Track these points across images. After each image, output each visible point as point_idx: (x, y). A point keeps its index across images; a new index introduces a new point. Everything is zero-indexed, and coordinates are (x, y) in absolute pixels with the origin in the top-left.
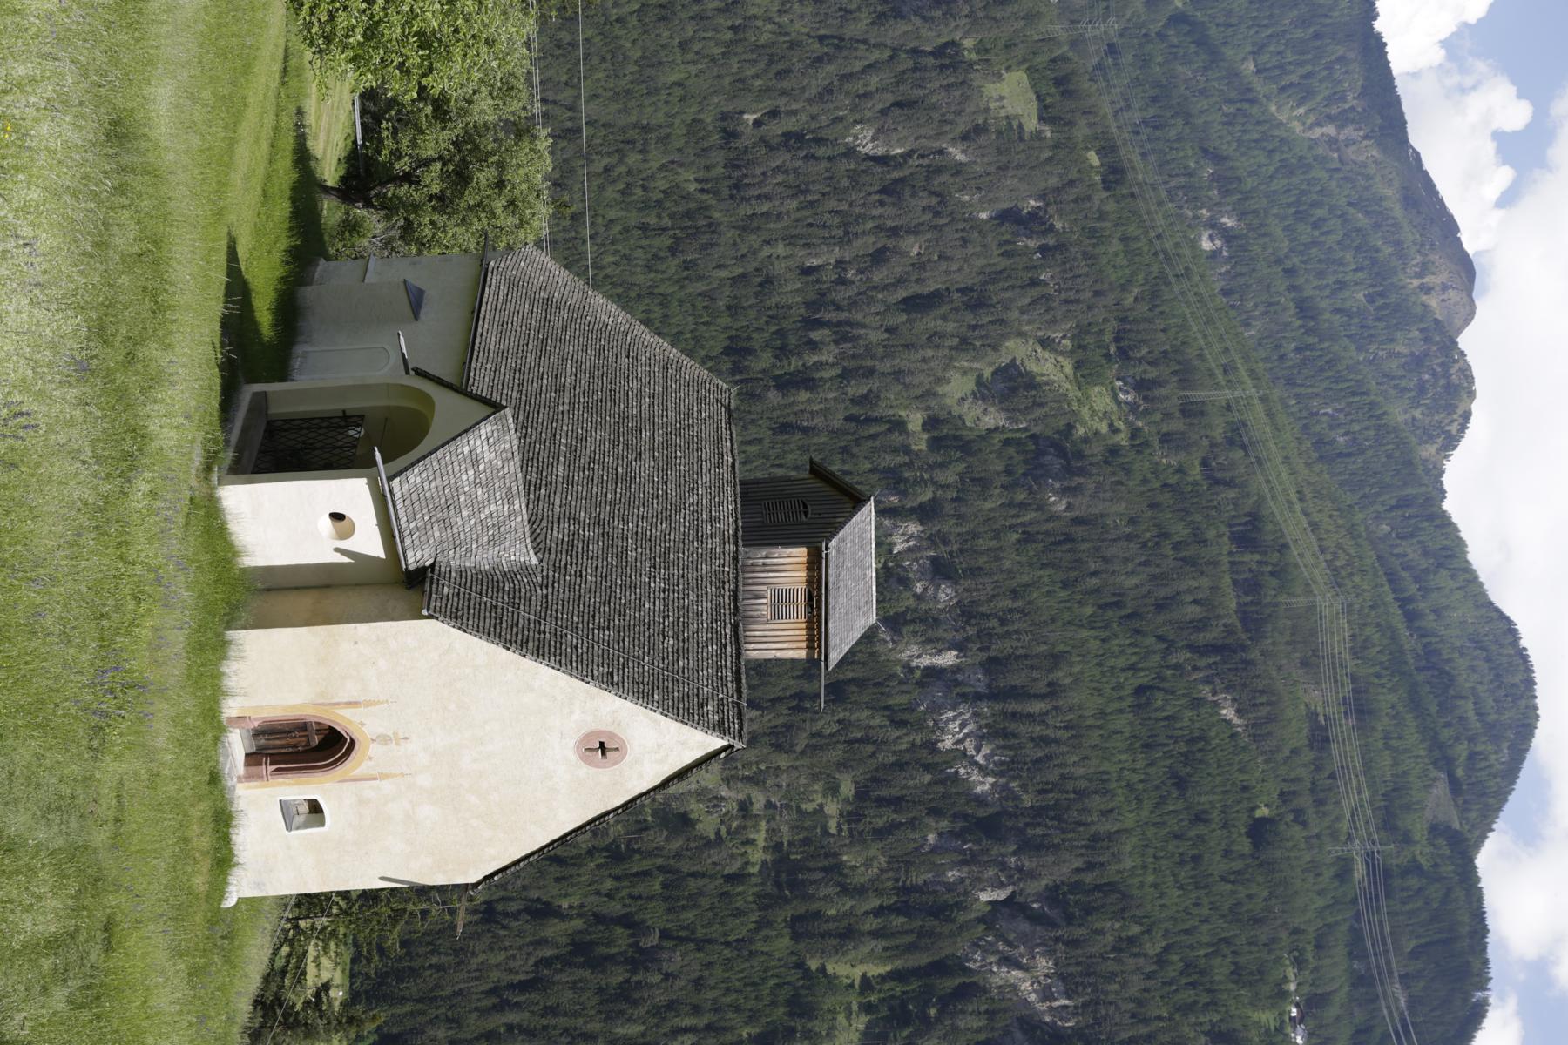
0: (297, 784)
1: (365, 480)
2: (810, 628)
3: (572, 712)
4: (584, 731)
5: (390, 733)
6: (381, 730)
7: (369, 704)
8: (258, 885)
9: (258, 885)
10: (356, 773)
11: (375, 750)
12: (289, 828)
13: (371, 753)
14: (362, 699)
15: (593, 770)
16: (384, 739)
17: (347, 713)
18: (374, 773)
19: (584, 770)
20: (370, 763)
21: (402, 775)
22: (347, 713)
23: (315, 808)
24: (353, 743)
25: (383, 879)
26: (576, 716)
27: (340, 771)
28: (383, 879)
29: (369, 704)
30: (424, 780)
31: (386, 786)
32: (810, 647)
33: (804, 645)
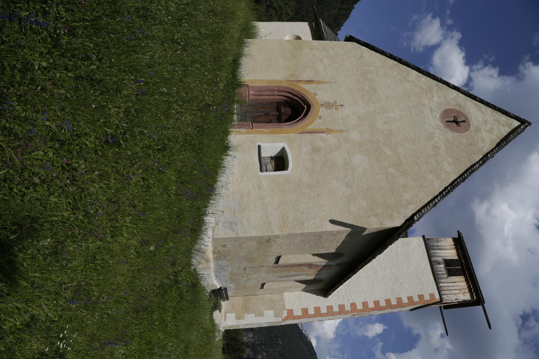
0: (272, 133)
1: (307, 23)
2: (466, 280)
3: (433, 96)
4: (443, 109)
5: (332, 102)
6: (326, 99)
7: (319, 82)
8: (231, 225)
9: (231, 225)
10: (311, 127)
11: (322, 112)
12: (261, 170)
13: (320, 114)
14: (315, 79)
15: (456, 134)
16: (328, 105)
17: (307, 87)
18: (324, 128)
19: (450, 135)
20: (320, 121)
21: (341, 131)
22: (307, 87)
23: (280, 162)
24: (309, 107)
25: (333, 222)
26: (435, 99)
27: (301, 124)
28: (333, 222)
29: (319, 82)
30: (355, 136)
31: (331, 138)
32: (470, 291)
33: (467, 291)
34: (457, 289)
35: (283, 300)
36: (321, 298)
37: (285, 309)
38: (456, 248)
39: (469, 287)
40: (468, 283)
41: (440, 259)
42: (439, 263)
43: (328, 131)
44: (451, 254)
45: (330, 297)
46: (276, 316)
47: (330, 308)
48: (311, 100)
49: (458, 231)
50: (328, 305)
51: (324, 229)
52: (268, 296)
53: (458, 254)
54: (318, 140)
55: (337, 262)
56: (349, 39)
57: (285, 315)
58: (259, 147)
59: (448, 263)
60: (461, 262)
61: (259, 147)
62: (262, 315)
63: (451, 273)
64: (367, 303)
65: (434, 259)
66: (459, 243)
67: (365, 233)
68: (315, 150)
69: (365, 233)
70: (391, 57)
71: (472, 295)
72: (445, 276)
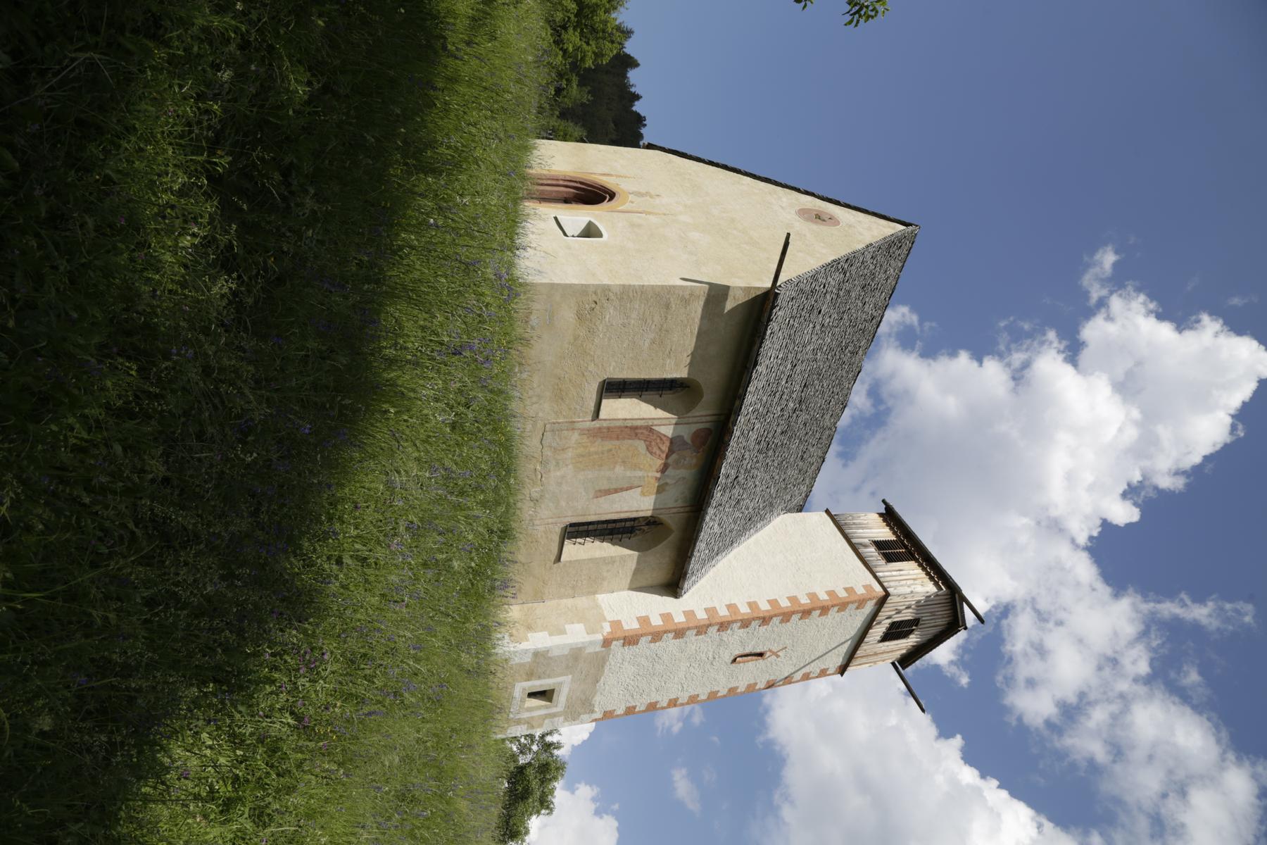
2: (920, 565)
6: (635, 189)
7: (618, 176)
32: (931, 578)
34: (910, 583)
35: (598, 606)
36: (669, 601)
37: (605, 620)
38: (888, 525)
39: (928, 574)
40: (924, 569)
41: (866, 541)
42: (865, 546)
43: (650, 213)
44: (885, 533)
45: (685, 597)
46: (590, 631)
47: (689, 614)
48: (614, 189)
49: (884, 501)
50: (686, 609)
51: (671, 283)
52: (569, 602)
53: (895, 533)
54: (635, 218)
55: (694, 428)
56: (650, 146)
57: (607, 629)
58: (556, 218)
59: (880, 545)
60: (902, 542)
61: (556, 218)
62: (562, 632)
63: (890, 558)
64: (755, 603)
65: (854, 541)
66: (890, 516)
67: (729, 305)
68: (633, 225)
69: (729, 305)
70: (711, 163)
71: (936, 584)
72: (883, 562)
